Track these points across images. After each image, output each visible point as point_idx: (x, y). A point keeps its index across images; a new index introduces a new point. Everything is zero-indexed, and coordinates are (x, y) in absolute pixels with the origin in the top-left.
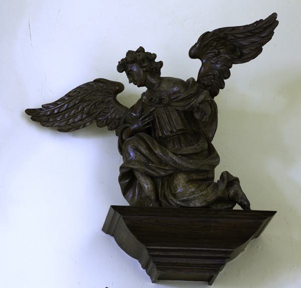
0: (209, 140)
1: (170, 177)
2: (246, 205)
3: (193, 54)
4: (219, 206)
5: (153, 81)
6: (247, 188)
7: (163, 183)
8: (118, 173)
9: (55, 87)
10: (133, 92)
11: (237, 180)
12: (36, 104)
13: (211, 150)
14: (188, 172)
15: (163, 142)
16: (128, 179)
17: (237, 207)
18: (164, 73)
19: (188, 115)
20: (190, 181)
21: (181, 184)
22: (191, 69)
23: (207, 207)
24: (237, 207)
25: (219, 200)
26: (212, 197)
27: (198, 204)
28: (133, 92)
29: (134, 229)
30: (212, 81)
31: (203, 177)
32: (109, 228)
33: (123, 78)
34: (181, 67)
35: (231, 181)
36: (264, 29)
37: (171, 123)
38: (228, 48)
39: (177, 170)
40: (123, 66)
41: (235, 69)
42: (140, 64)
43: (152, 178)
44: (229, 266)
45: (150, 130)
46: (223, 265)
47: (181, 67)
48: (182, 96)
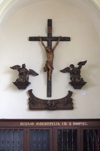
0: (80, 74)
1: (76, 78)
2: (84, 81)
3: (78, 65)
4: (81, 82)
5: (73, 68)
6: (84, 79)
7: (75, 79)
8: (70, 78)
9: (63, 68)
10: (71, 69)
11: (83, 79)
12: (61, 70)
13: (80, 75)
14: (77, 78)
15: (75, 75)
16: (71, 79)
17: (83, 82)
18: (75, 67)
19: (77, 72)
20: (78, 79)
21: (77, 79)
22: (77, 66)
23: (79, 82)
24: (83, 82)
25: (81, 81)
26: (80, 81)
27: (79, 81)
28: (71, 69)
29: (71, 84)
30: (80, 68)
31: (79, 78)
32: (69, 84)
33: (70, 67)
34: (76, 66)
35: (82, 79)
36: (85, 62)
37: (76, 73)
38: (82, 64)
39: (76, 78)
40: (70, 66)
41: (82, 66)
42: (72, 66)
43: (74, 79)
44: (82, 87)
45: (73, 73)
46: (81, 88)
47: (76, 66)
48: (77, 69)
